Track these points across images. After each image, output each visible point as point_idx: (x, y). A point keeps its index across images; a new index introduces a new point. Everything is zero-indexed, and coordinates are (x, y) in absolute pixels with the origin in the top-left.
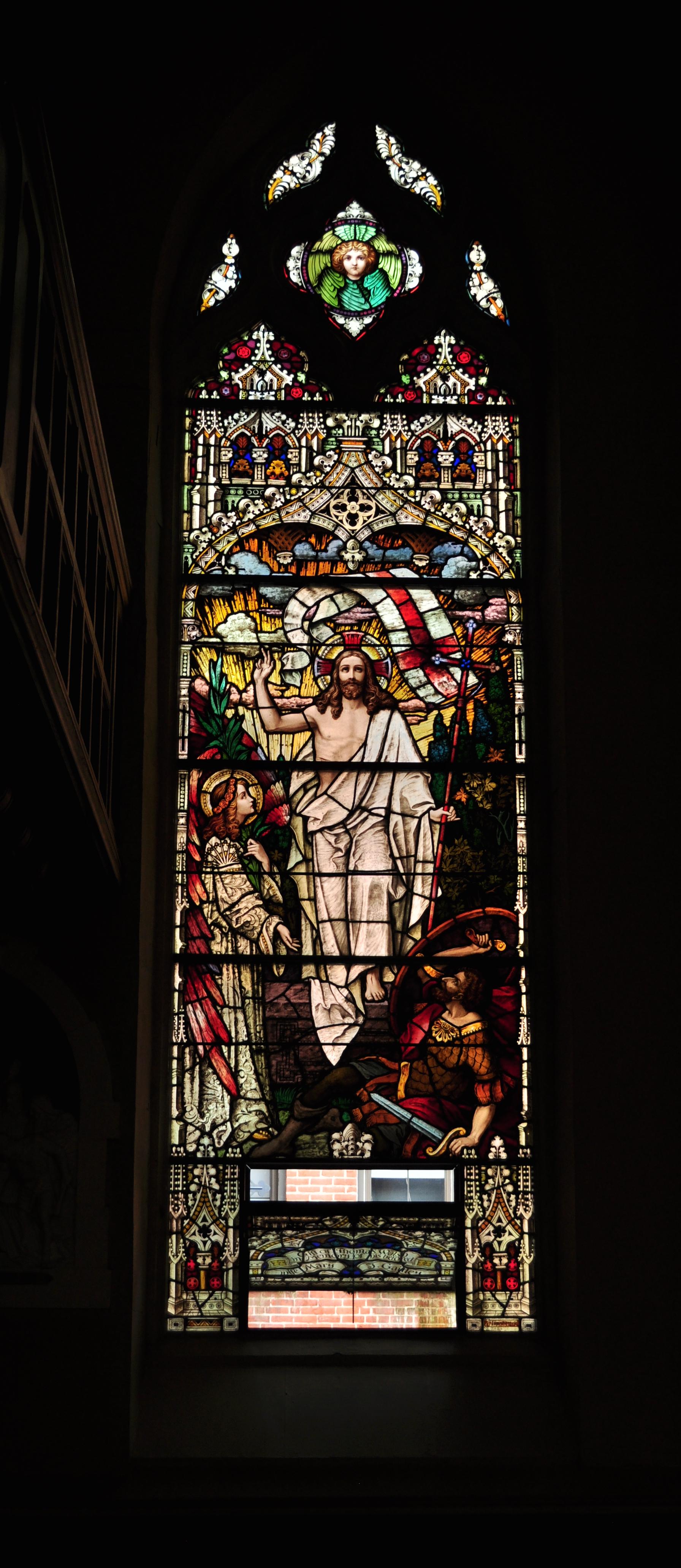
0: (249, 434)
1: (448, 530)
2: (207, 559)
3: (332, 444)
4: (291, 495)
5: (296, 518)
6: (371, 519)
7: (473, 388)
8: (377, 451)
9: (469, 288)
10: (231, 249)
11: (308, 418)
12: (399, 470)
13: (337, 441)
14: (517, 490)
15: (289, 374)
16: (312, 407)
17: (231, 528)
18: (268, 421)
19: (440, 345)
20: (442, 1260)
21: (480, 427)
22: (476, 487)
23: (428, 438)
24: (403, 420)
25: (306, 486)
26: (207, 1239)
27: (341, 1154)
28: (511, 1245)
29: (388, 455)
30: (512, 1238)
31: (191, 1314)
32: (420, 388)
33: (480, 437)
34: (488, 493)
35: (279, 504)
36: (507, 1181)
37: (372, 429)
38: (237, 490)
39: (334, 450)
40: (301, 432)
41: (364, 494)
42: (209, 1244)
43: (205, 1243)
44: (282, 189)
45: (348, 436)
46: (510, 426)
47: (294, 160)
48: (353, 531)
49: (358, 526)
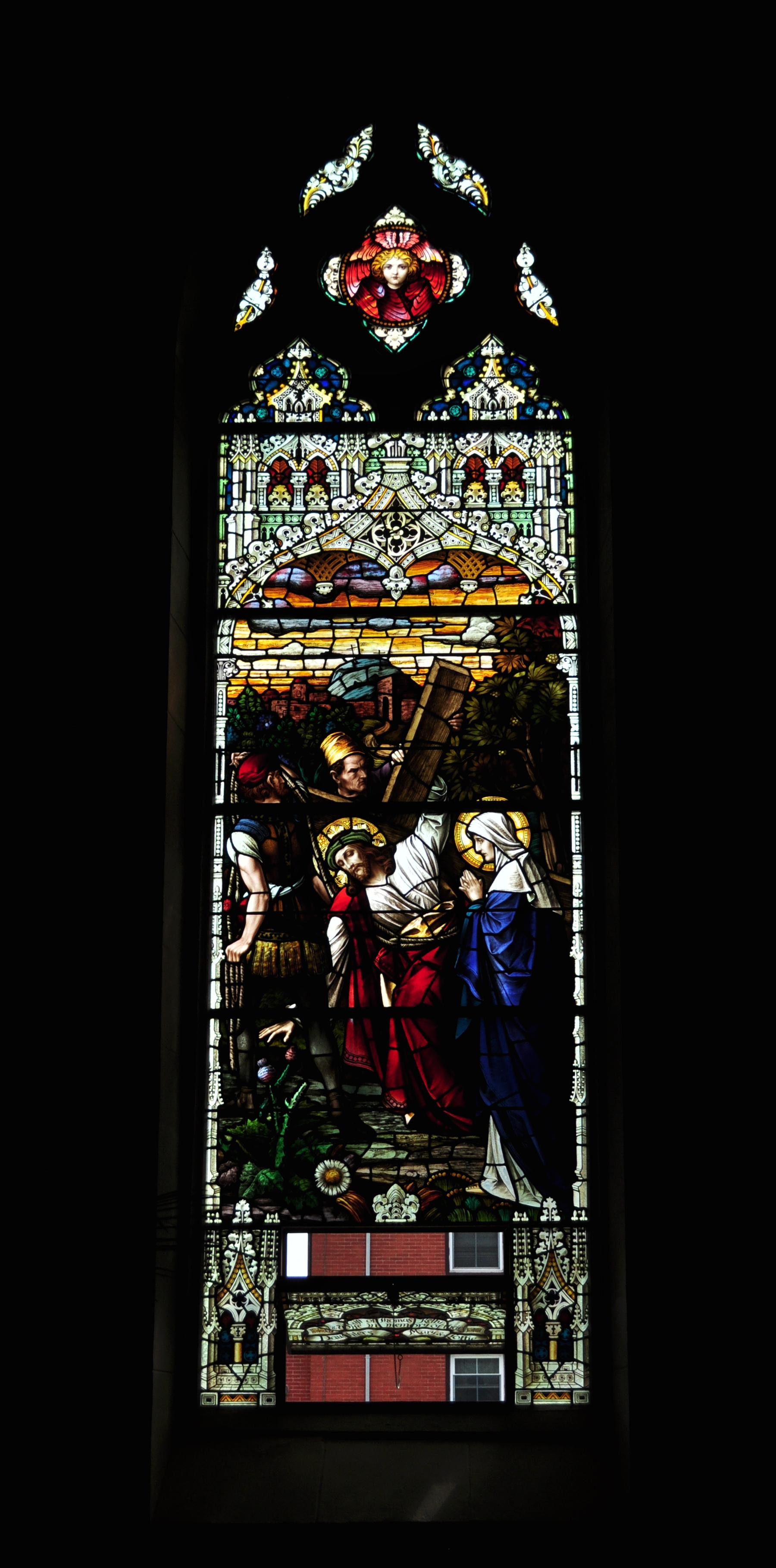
0: (287, 458)
1: (497, 552)
2: (243, 592)
3: (374, 465)
4: (332, 521)
5: (337, 546)
6: (416, 544)
7: (523, 401)
8: (421, 472)
9: (520, 294)
10: (265, 263)
11: (349, 439)
12: (443, 491)
13: (379, 462)
14: (570, 507)
15: (327, 394)
16: (352, 428)
17: (269, 558)
18: (308, 444)
19: (488, 357)
20: (492, 1327)
21: (530, 441)
22: (526, 505)
23: (475, 456)
24: (448, 438)
25: (348, 511)
26: (241, 1308)
27: (385, 1218)
28: (564, 1311)
29: (433, 476)
30: (565, 1304)
31: (225, 1389)
32: (467, 403)
33: (530, 451)
34: (539, 510)
35: (320, 530)
36: (560, 1244)
37: (415, 448)
38: (275, 516)
39: (376, 471)
40: (342, 454)
41: (407, 517)
42: (243, 1314)
43: (239, 1312)
44: (318, 198)
45: (391, 457)
46: (562, 440)
47: (330, 167)
48: (397, 557)
49: (402, 553)
